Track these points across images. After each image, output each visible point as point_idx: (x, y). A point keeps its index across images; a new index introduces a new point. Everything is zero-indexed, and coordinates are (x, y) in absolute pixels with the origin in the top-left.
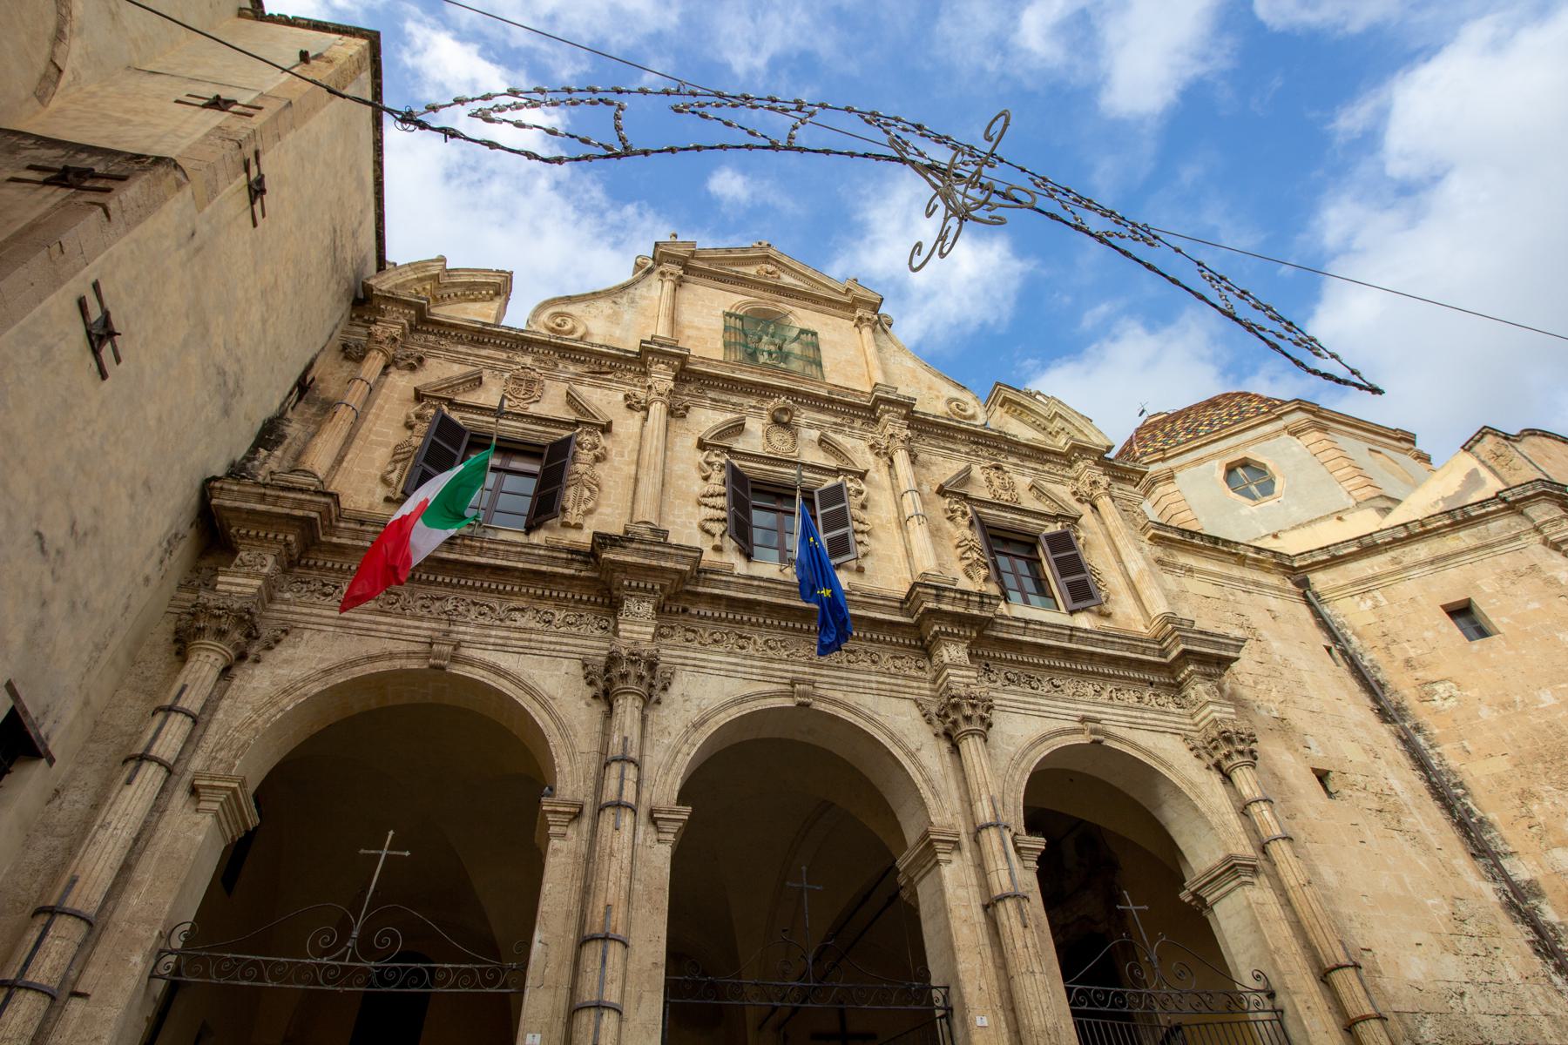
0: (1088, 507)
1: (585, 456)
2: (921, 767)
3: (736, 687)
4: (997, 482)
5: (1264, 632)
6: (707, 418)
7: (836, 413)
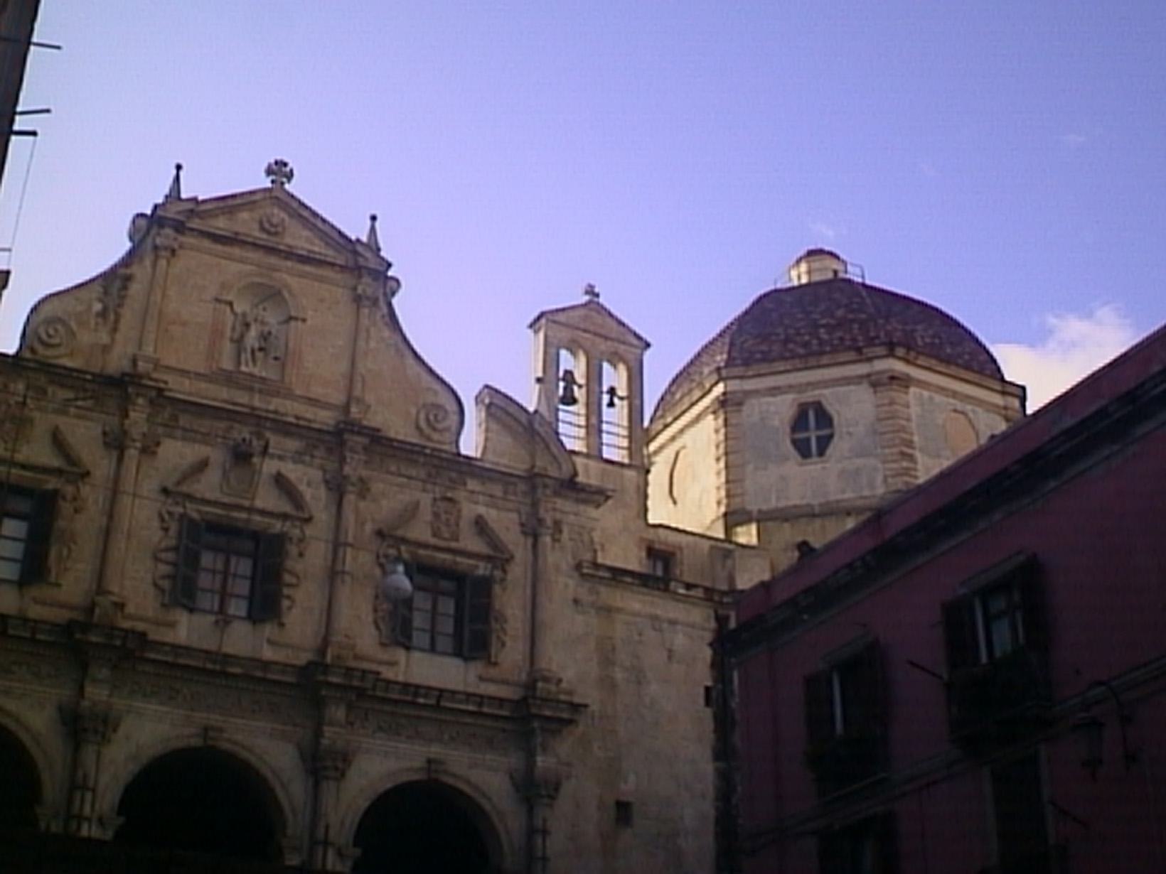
1: (66, 507)
6: (176, 453)
7: (301, 437)
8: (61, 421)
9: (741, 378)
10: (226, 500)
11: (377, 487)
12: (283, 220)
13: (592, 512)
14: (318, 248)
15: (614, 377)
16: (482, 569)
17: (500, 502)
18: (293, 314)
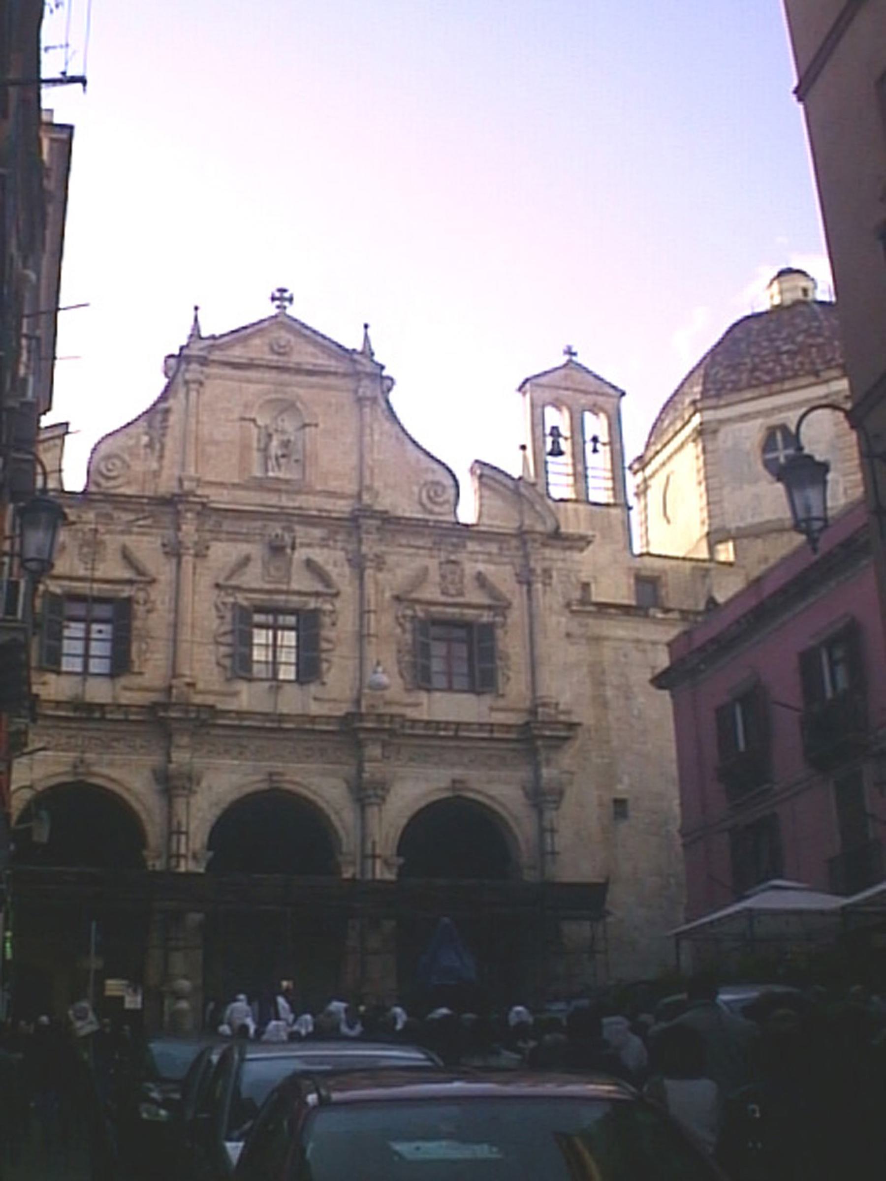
0: (525, 588)
1: (140, 610)
2: (341, 820)
3: (236, 778)
5: (636, 689)
6: (224, 553)
7: (323, 526)
8: (127, 539)
9: (715, 408)
10: (267, 586)
11: (391, 559)
12: (289, 341)
13: (577, 556)
14: (323, 361)
15: (596, 425)
16: (486, 617)
17: (497, 559)
18: (307, 421)
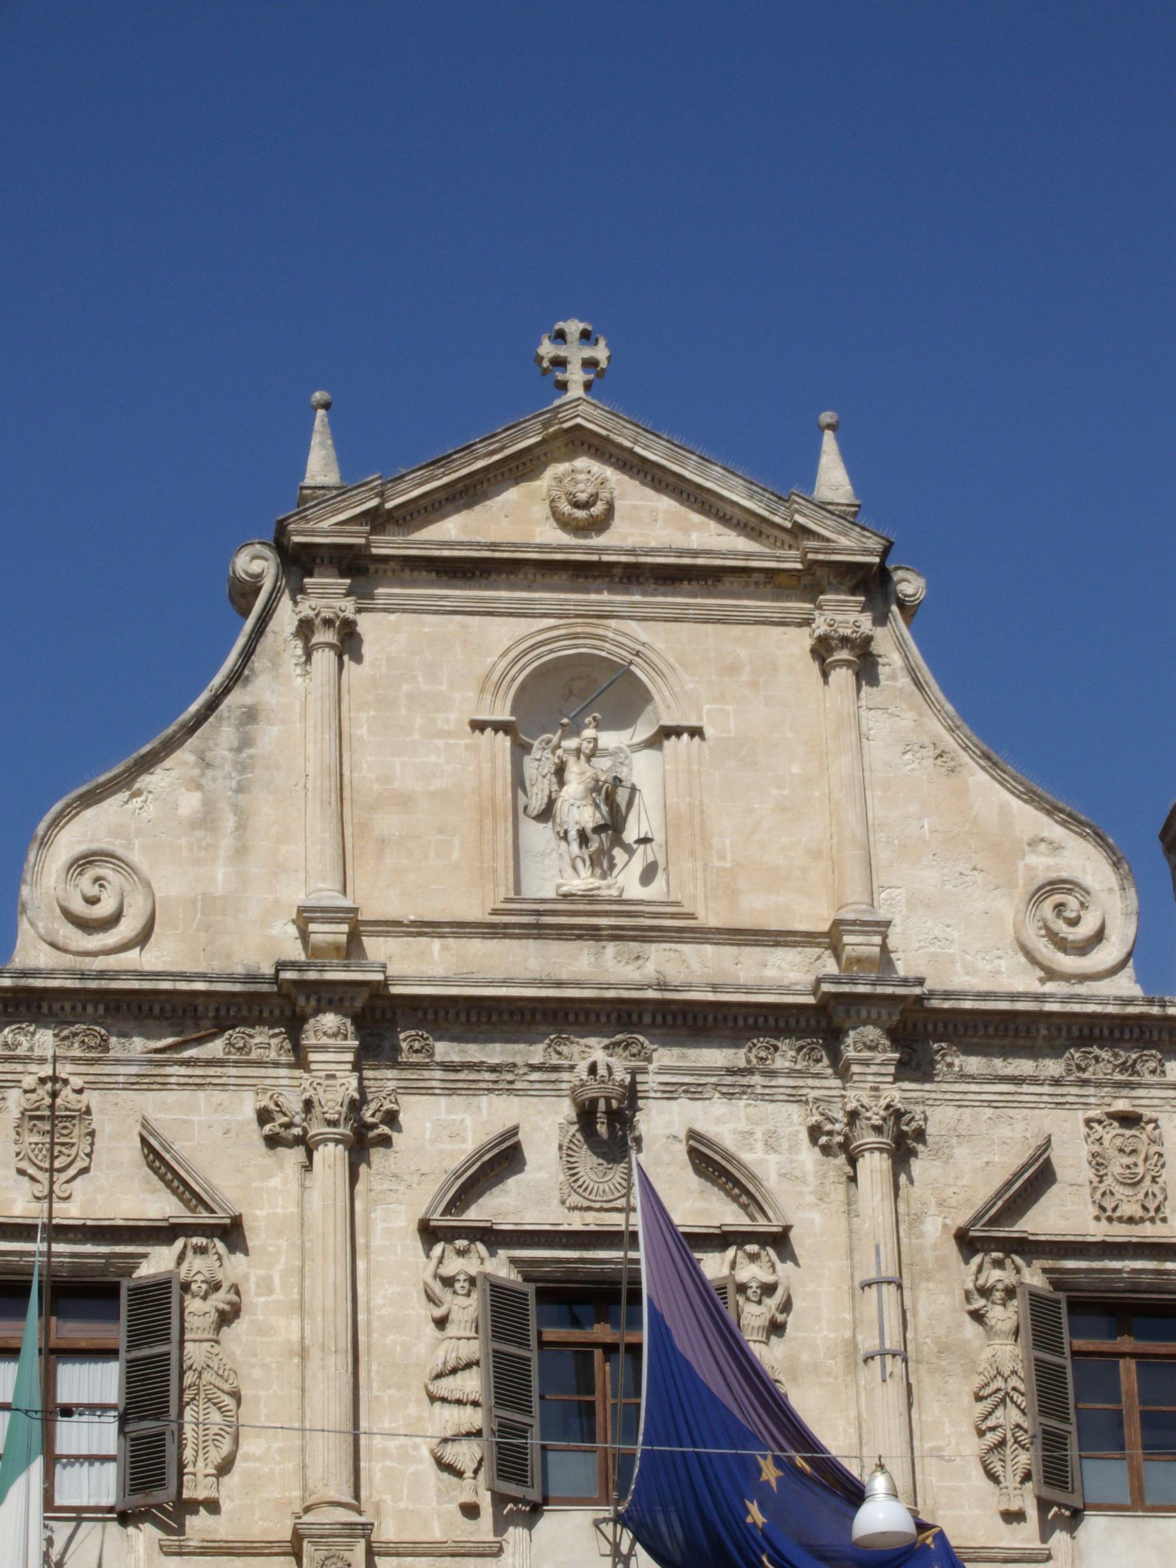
1: (199, 1311)
4: (1117, 1165)
6: (439, 1129)
10: (575, 1222)
